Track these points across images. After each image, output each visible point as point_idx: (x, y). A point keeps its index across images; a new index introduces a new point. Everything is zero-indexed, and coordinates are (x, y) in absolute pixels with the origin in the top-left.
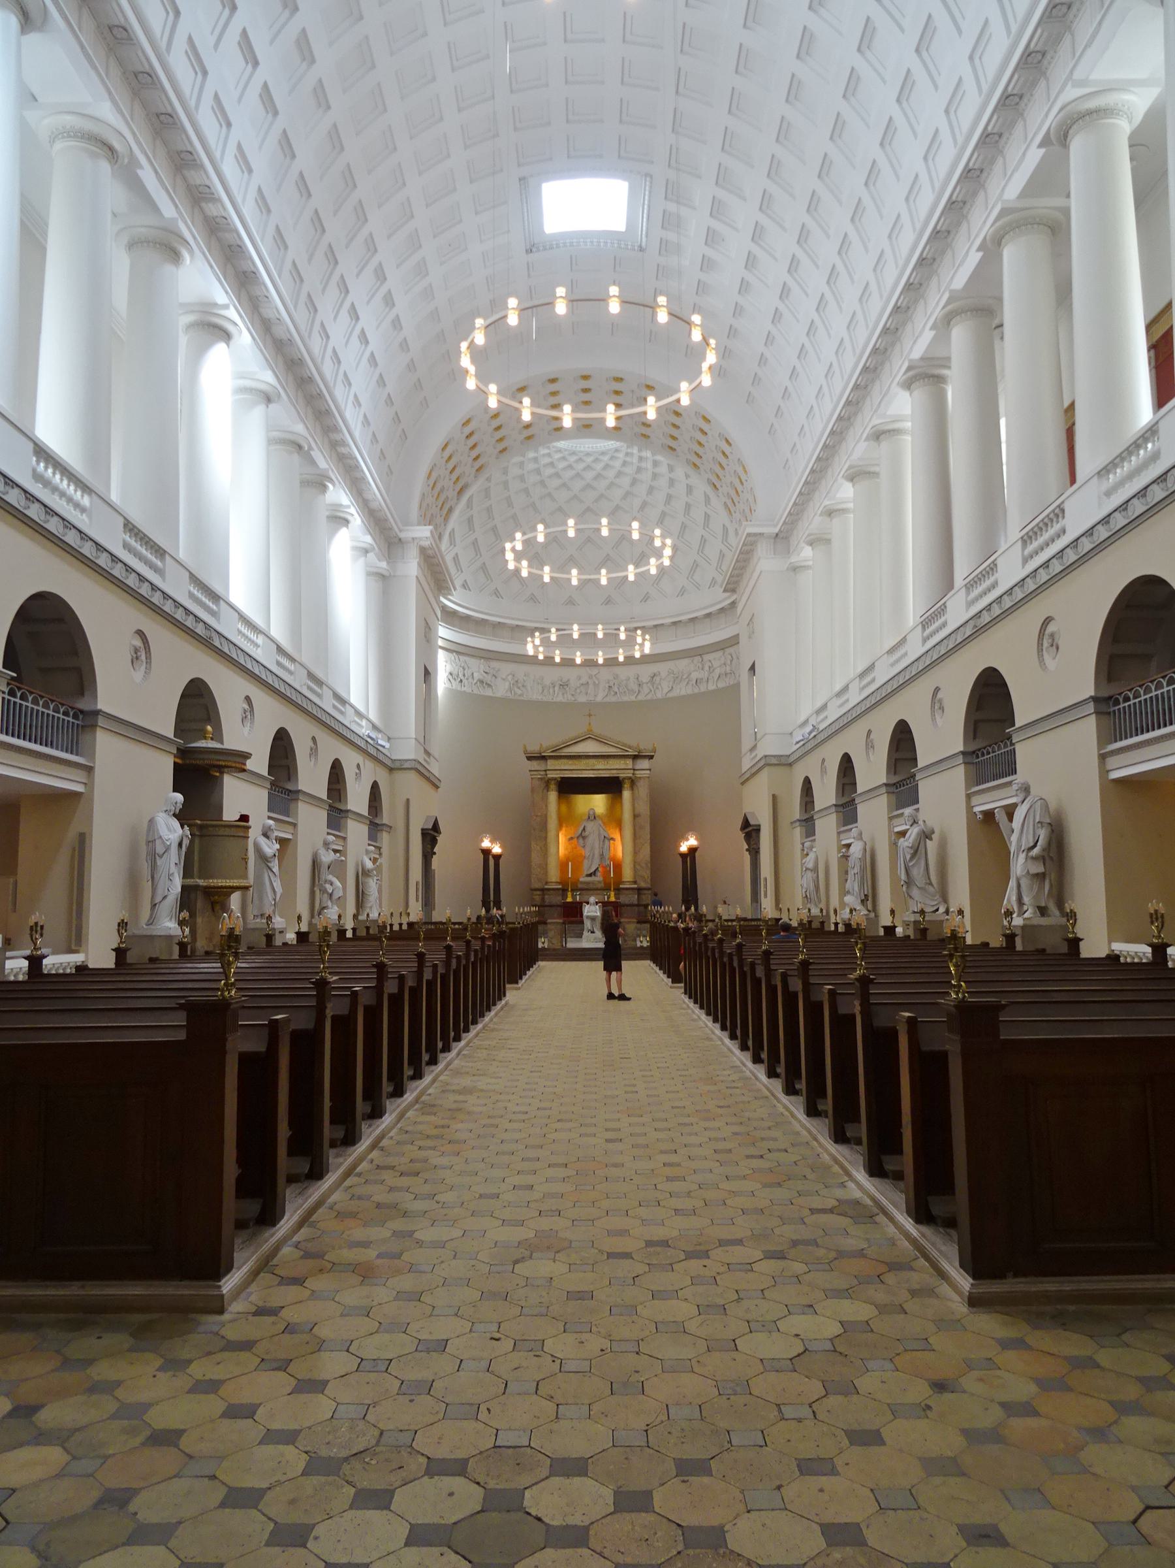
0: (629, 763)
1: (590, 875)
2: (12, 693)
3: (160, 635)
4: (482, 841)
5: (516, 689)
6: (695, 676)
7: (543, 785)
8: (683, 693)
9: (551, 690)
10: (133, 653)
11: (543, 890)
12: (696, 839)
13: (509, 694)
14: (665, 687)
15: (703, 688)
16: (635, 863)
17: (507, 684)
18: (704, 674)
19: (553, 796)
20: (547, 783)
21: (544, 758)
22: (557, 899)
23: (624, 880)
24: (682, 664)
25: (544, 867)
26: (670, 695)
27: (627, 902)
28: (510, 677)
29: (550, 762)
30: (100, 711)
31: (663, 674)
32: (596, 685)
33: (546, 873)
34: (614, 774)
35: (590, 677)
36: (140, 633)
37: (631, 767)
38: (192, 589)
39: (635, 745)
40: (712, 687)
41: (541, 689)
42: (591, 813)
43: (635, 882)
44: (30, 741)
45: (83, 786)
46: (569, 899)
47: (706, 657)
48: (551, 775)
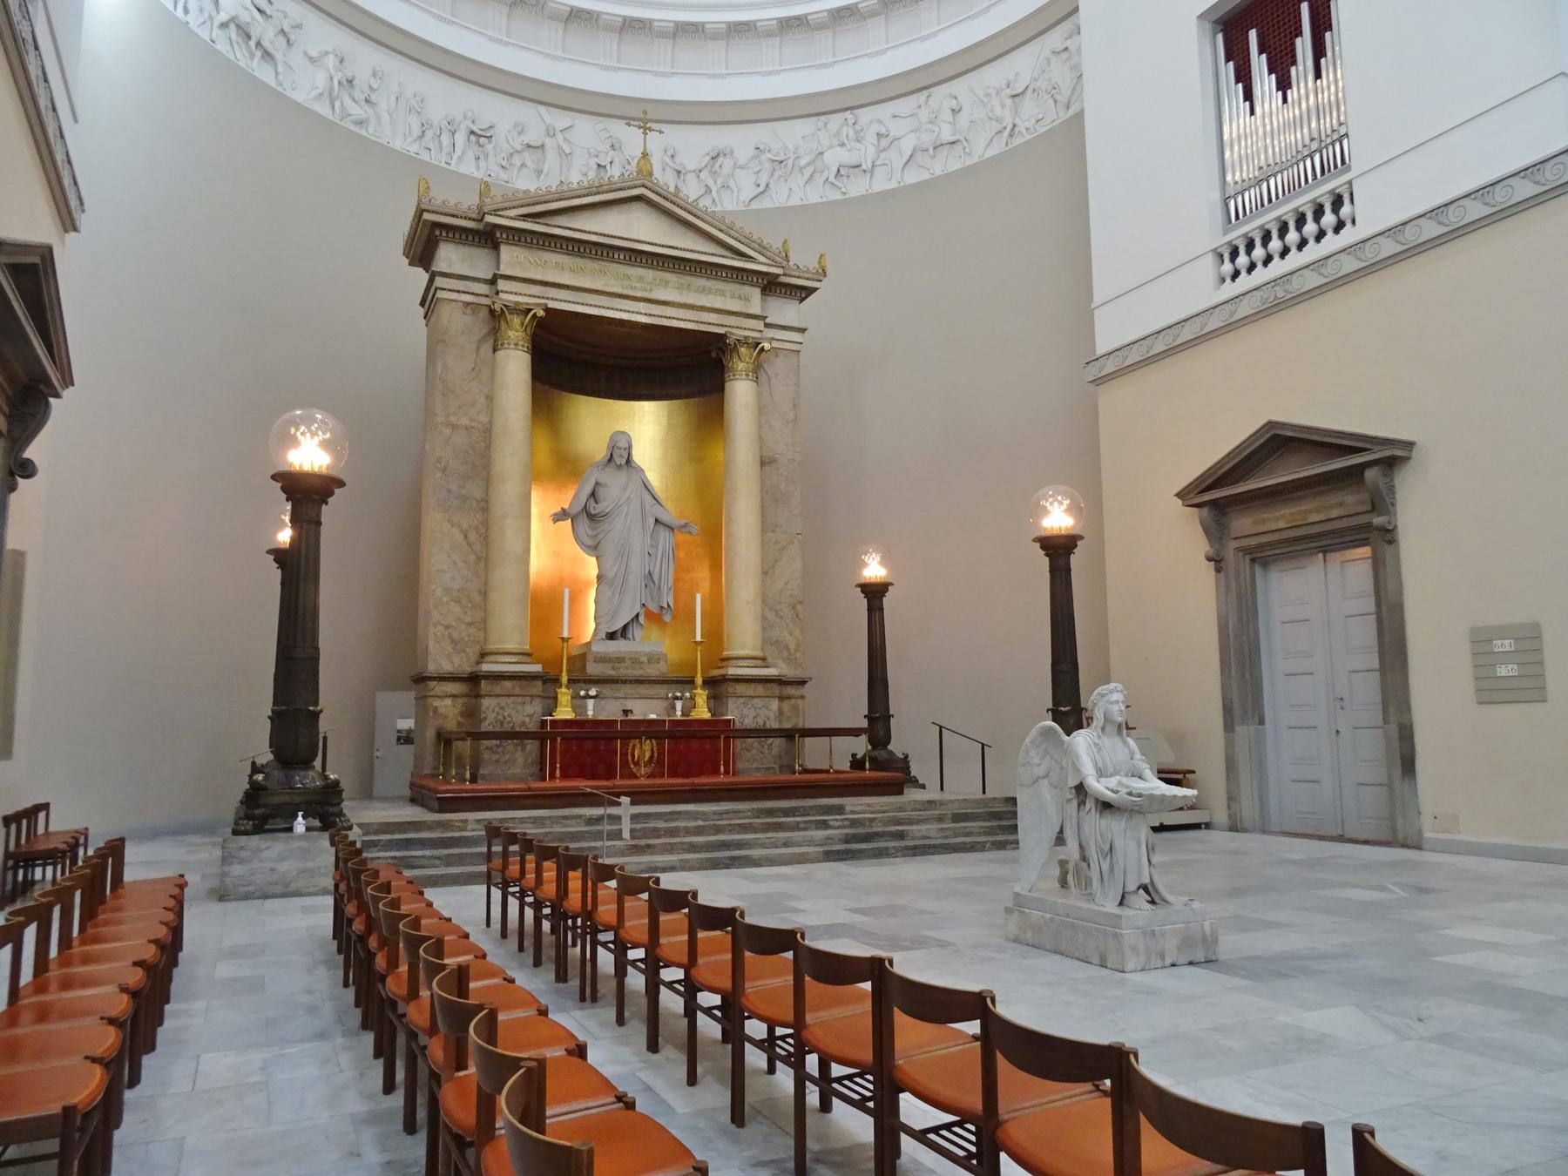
0: (753, 300)
1: (611, 636)
4: (293, 442)
5: (348, 101)
6: (835, 157)
7: (480, 326)
8: (795, 201)
9: (445, 138)
11: (473, 679)
12: (1073, 510)
13: (323, 109)
14: (745, 186)
15: (857, 187)
16: (766, 601)
17: (321, 80)
18: (865, 153)
19: (515, 366)
20: (497, 317)
21: (487, 237)
22: (524, 712)
23: (726, 653)
24: (794, 135)
25: (480, 598)
26: (765, 203)
27: (749, 723)
28: (331, 61)
29: (506, 252)
31: (743, 155)
32: (565, 156)
33: (483, 625)
34: (709, 323)
35: (550, 132)
37: (756, 310)
39: (776, 244)
40: (881, 184)
41: (416, 132)
42: (623, 444)
43: (763, 661)
46: (564, 712)
47: (864, 115)
48: (511, 294)
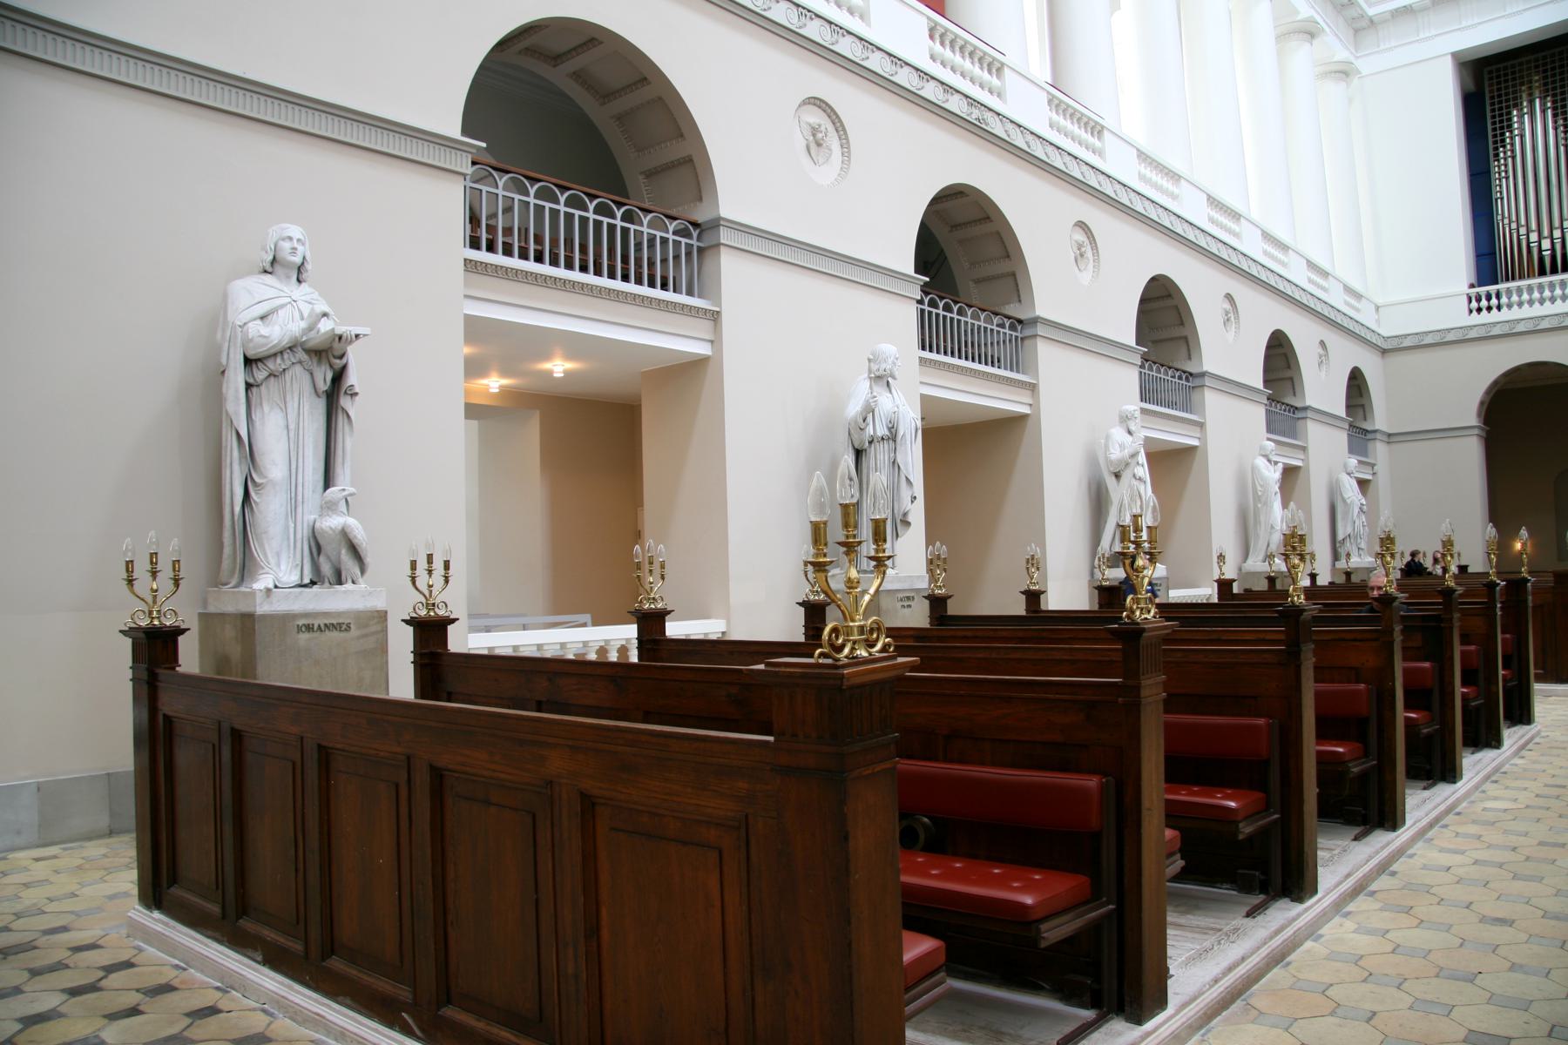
2: (933, 304)
3: (1102, 221)
10: (1075, 249)
30: (1038, 317)
36: (1082, 225)
38: (1143, 171)
44: (931, 351)
45: (1028, 407)
